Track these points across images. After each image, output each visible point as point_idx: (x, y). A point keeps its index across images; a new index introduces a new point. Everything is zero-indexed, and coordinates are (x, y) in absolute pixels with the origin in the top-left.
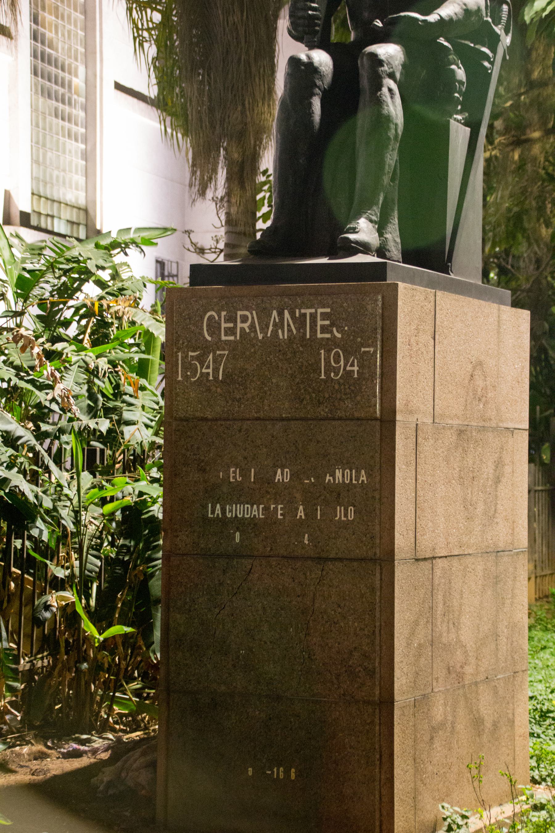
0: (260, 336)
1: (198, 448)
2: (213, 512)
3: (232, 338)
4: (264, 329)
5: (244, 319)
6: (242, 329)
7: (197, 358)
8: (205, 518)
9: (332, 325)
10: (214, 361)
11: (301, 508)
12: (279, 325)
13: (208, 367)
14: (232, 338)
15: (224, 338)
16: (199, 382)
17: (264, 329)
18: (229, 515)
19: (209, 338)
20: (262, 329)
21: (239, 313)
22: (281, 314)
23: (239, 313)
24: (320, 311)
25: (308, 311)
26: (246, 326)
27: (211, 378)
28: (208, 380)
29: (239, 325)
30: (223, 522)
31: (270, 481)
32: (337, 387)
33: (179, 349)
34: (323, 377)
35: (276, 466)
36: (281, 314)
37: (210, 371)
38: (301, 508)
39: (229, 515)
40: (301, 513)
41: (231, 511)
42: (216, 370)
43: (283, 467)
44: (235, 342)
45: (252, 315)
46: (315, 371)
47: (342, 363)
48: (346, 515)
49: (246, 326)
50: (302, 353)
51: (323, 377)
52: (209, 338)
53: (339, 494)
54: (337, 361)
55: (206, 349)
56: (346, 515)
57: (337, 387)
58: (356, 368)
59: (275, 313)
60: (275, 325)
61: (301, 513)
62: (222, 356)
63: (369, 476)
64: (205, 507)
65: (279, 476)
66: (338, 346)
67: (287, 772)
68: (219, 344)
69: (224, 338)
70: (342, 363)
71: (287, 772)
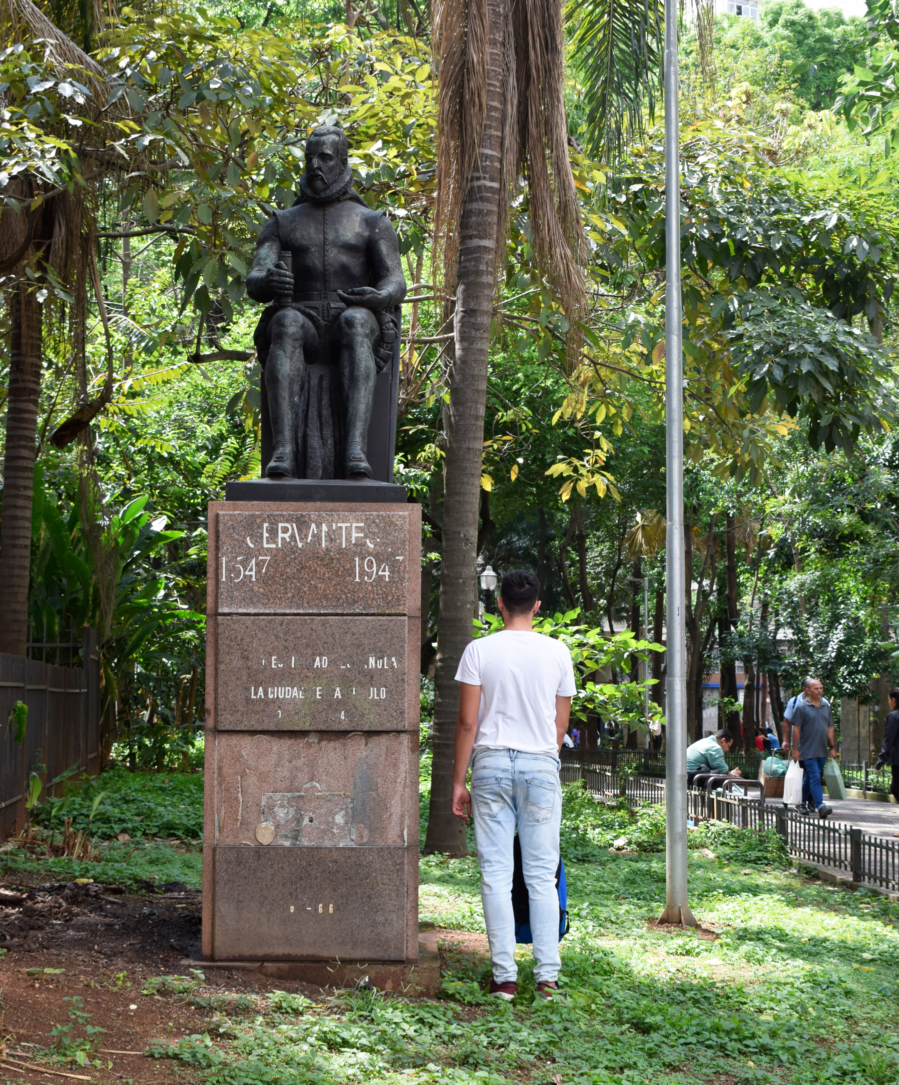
0: (300, 545)
1: (242, 639)
2: (256, 694)
3: (274, 546)
4: (303, 538)
5: (285, 530)
6: (283, 539)
7: (241, 562)
8: (248, 700)
9: (366, 536)
10: (257, 565)
11: (338, 689)
12: (317, 537)
13: (251, 570)
14: (274, 546)
15: (265, 546)
16: (243, 582)
17: (303, 538)
18: (271, 696)
19: (252, 546)
20: (301, 539)
21: (280, 525)
22: (319, 526)
23: (280, 525)
24: (354, 525)
25: (344, 525)
26: (286, 536)
27: (254, 579)
28: (251, 582)
29: (280, 535)
30: (266, 702)
31: (310, 667)
32: (370, 588)
33: (224, 554)
34: (357, 580)
35: (314, 655)
36: (319, 526)
37: (253, 573)
38: (338, 689)
39: (271, 696)
40: (338, 694)
41: (273, 693)
42: (258, 572)
43: (321, 655)
44: (277, 549)
45: (292, 527)
46: (350, 575)
47: (375, 569)
48: (378, 695)
49: (286, 536)
50: (338, 559)
51: (357, 580)
52: (252, 546)
53: (371, 678)
54: (370, 567)
55: (249, 555)
56: (378, 695)
57: (370, 588)
58: (387, 573)
59: (313, 526)
60: (314, 536)
61: (338, 694)
62: (264, 561)
63: (399, 662)
64: (249, 690)
65: (317, 663)
66: (370, 554)
67: (326, 907)
68: (260, 551)
69: (265, 546)
70: (375, 569)
71: (326, 907)
